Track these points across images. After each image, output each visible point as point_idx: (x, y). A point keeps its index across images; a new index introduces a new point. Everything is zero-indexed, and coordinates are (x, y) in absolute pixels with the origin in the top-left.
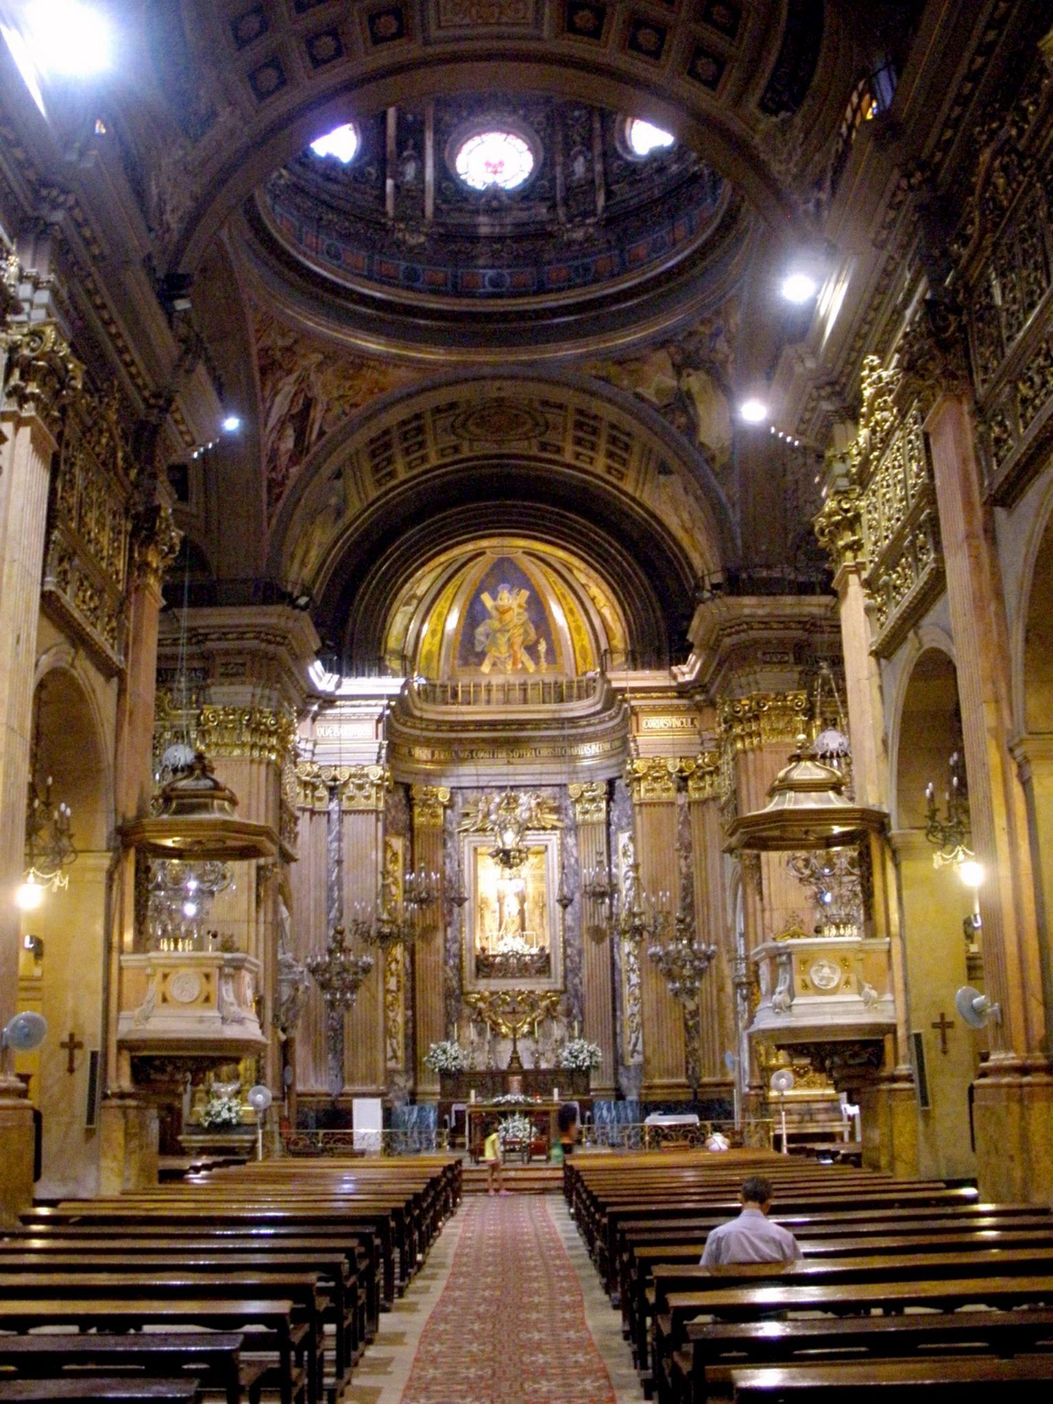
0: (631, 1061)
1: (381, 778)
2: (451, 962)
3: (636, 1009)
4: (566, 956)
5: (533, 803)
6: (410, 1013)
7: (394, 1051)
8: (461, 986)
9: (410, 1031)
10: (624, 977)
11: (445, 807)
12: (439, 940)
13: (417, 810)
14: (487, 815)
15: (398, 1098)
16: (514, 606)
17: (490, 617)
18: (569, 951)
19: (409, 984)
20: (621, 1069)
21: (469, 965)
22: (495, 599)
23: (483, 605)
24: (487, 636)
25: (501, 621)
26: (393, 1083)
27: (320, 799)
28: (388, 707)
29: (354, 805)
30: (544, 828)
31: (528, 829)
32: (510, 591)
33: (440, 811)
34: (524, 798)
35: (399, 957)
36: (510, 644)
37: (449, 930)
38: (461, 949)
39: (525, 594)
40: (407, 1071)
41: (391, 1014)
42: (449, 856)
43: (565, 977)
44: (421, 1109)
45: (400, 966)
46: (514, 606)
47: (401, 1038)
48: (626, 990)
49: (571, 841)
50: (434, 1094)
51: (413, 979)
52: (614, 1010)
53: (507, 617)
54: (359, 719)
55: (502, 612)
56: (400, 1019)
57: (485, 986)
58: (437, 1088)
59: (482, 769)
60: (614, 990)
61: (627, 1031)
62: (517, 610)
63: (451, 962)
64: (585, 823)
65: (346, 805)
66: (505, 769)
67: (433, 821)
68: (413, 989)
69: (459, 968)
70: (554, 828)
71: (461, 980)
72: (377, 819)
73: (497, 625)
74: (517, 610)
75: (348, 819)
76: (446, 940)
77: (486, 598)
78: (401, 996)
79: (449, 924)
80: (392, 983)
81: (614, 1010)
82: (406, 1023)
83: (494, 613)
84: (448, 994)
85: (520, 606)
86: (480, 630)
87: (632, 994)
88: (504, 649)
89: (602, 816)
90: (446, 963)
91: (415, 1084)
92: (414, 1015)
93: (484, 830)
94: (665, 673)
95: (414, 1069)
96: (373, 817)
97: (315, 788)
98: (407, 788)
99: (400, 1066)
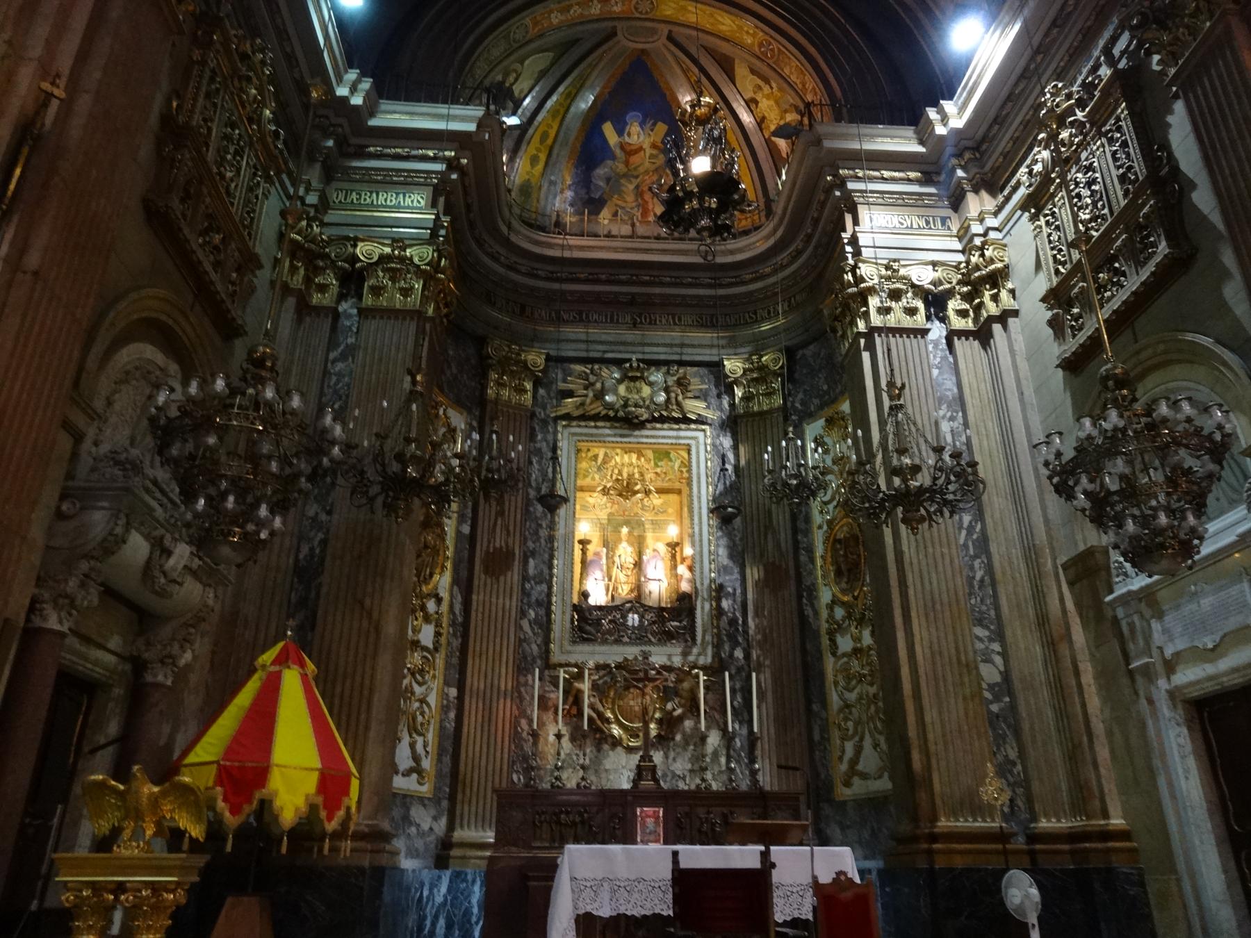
0: (843, 793)
1: (435, 265)
2: (532, 614)
3: (852, 697)
4: (719, 612)
5: (671, 381)
6: (453, 692)
7: (416, 758)
8: (547, 652)
9: (450, 726)
10: (825, 641)
11: (537, 383)
12: (514, 576)
13: (494, 376)
14: (599, 396)
15: (414, 853)
16: (646, 146)
17: (614, 158)
18: (725, 604)
19: (456, 643)
20: (827, 810)
21: (561, 620)
22: (620, 132)
23: (605, 141)
24: (608, 180)
25: (627, 163)
26: (407, 820)
27: (323, 288)
28: (452, 165)
29: (383, 302)
30: (686, 420)
31: (662, 420)
32: (642, 125)
33: (528, 386)
34: (657, 376)
35: (445, 594)
36: (639, 193)
37: (532, 562)
38: (549, 595)
39: (662, 128)
40: (436, 800)
41: (418, 690)
42: (538, 452)
43: (717, 647)
44: (458, 876)
45: (444, 607)
46: (646, 146)
47: (430, 736)
48: (830, 664)
49: (727, 442)
50: (483, 846)
51: (465, 636)
52: (809, 702)
53: (635, 159)
54: (407, 182)
55: (629, 151)
56: (432, 699)
57: (592, 655)
58: (490, 837)
59: (595, 332)
60: (806, 666)
61: (835, 735)
62: (649, 151)
63: (532, 614)
64: (749, 415)
65: (368, 300)
66: (631, 335)
67: (515, 398)
68: (464, 650)
69: (545, 625)
70: (701, 421)
71: (547, 641)
72: (420, 332)
73: (621, 168)
74: (649, 151)
75: (372, 325)
76: (525, 578)
77: (608, 129)
78: (440, 660)
79: (533, 554)
80: (427, 635)
81: (809, 702)
82: (445, 709)
83: (618, 152)
84: (522, 667)
85: (654, 146)
86: (601, 171)
87: (846, 669)
88: (630, 198)
89: (778, 401)
90: (523, 614)
91: (451, 827)
92: (460, 698)
93: (596, 418)
94: (909, 131)
95: (452, 798)
96: (413, 327)
97: (318, 271)
98: (481, 341)
99: (425, 789)
